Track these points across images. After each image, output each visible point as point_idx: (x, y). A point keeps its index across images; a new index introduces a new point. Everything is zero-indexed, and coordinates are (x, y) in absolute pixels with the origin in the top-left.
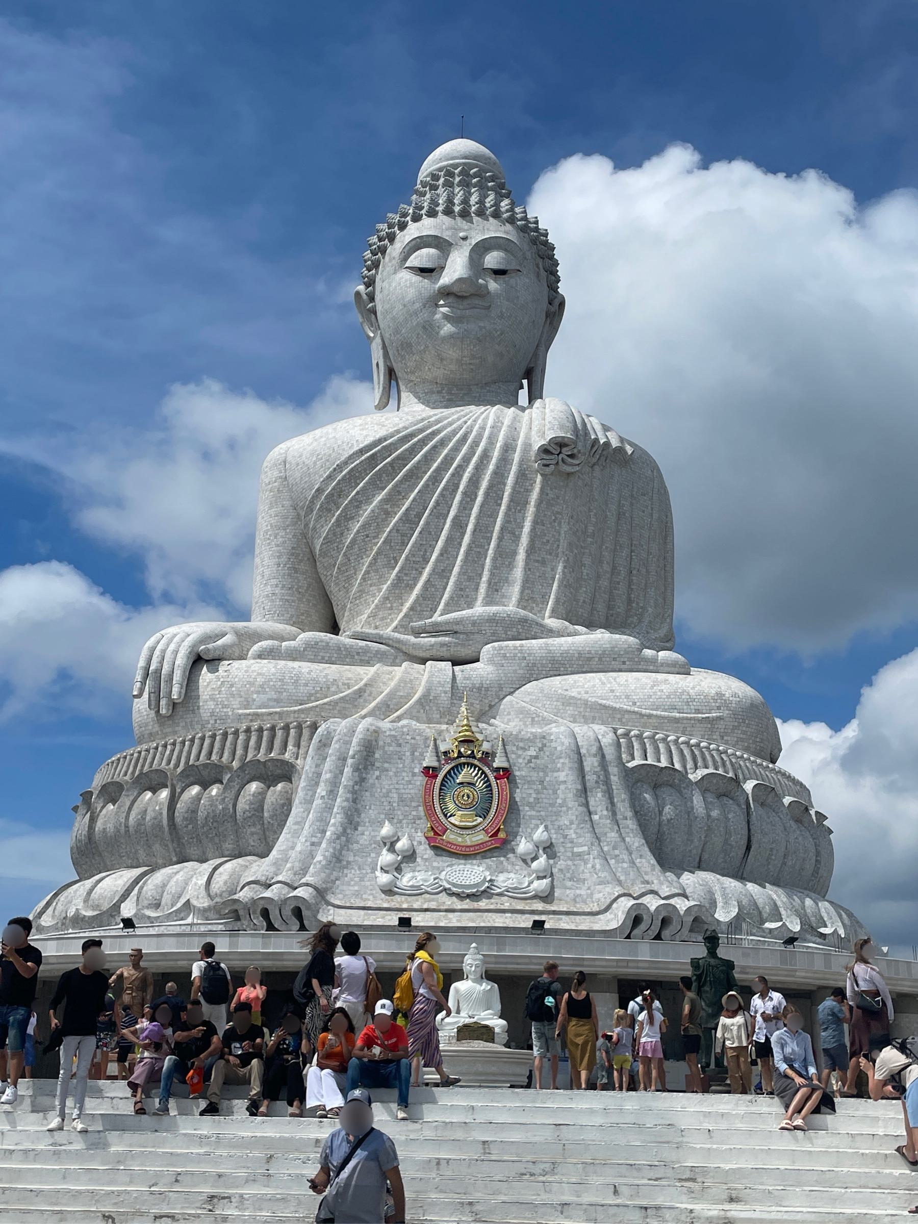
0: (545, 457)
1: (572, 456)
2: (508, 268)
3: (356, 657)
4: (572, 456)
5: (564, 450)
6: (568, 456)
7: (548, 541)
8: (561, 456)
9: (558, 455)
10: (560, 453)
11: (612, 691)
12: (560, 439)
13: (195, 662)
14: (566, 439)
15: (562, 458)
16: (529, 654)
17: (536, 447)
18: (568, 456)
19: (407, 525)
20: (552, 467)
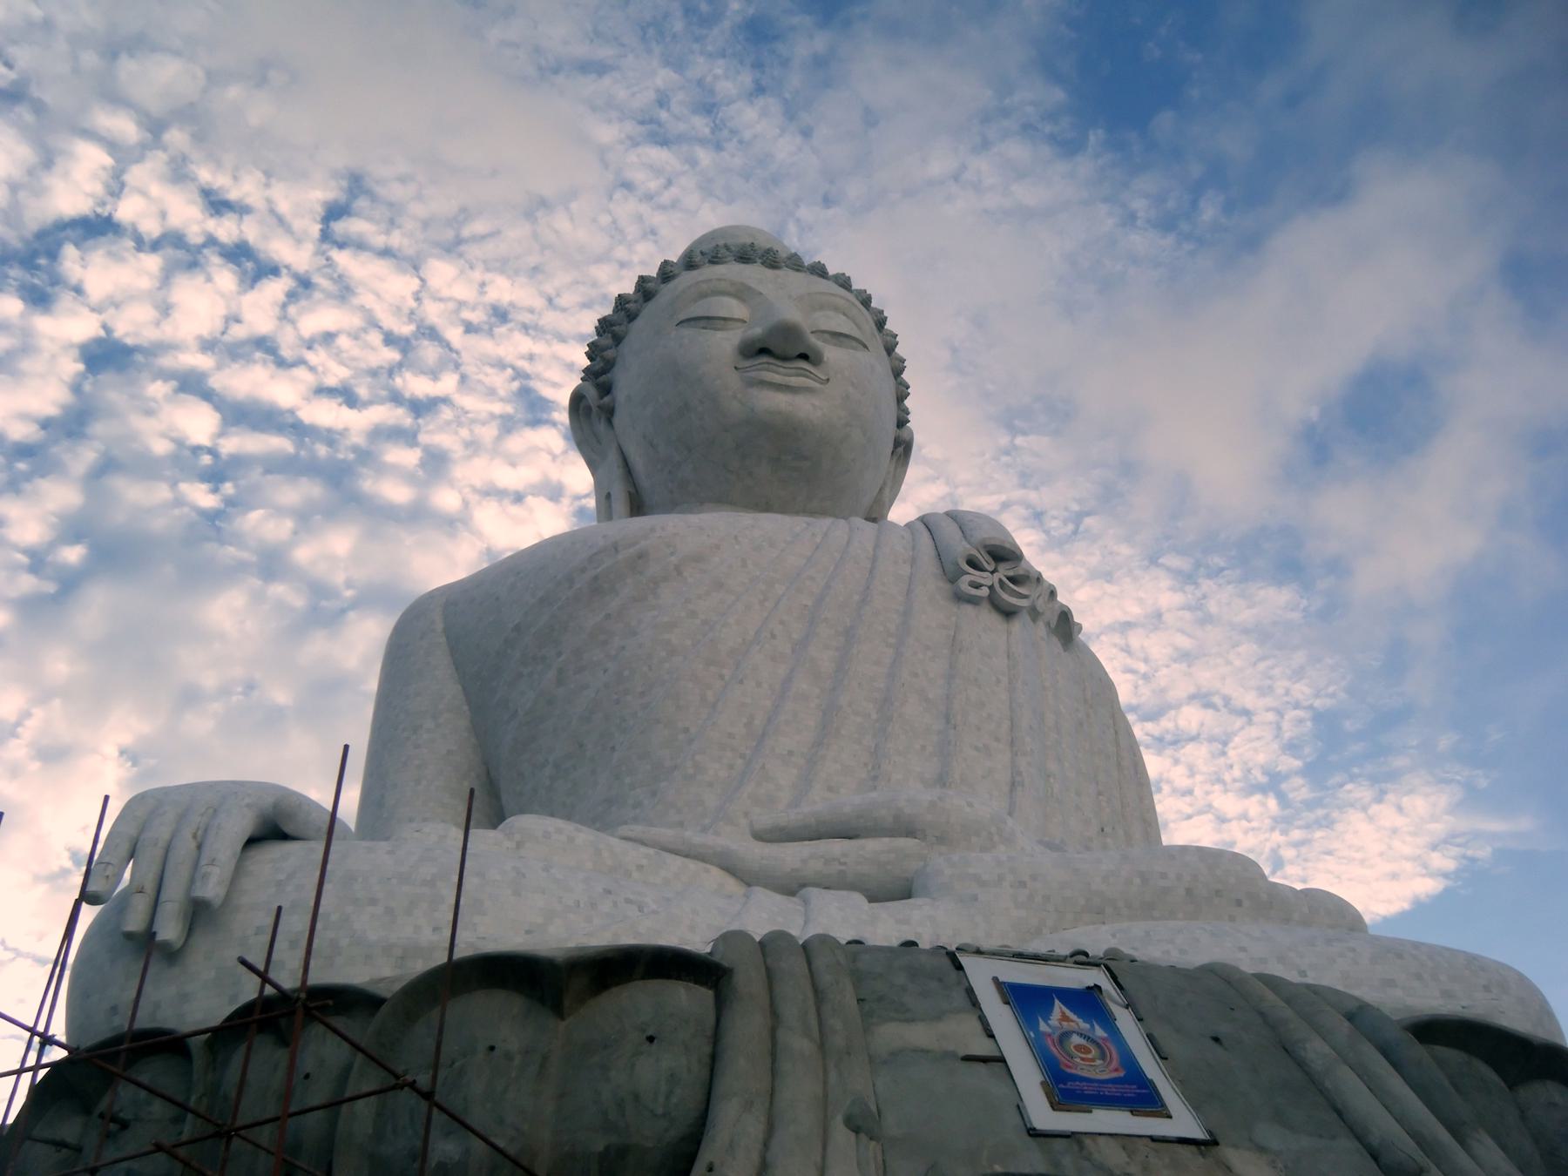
1: (1012, 580)
3: (636, 875)
4: (1012, 580)
6: (1011, 579)
9: (992, 573)
11: (1243, 949)
13: (252, 842)
15: (1000, 580)
16: (1034, 878)
18: (1011, 579)
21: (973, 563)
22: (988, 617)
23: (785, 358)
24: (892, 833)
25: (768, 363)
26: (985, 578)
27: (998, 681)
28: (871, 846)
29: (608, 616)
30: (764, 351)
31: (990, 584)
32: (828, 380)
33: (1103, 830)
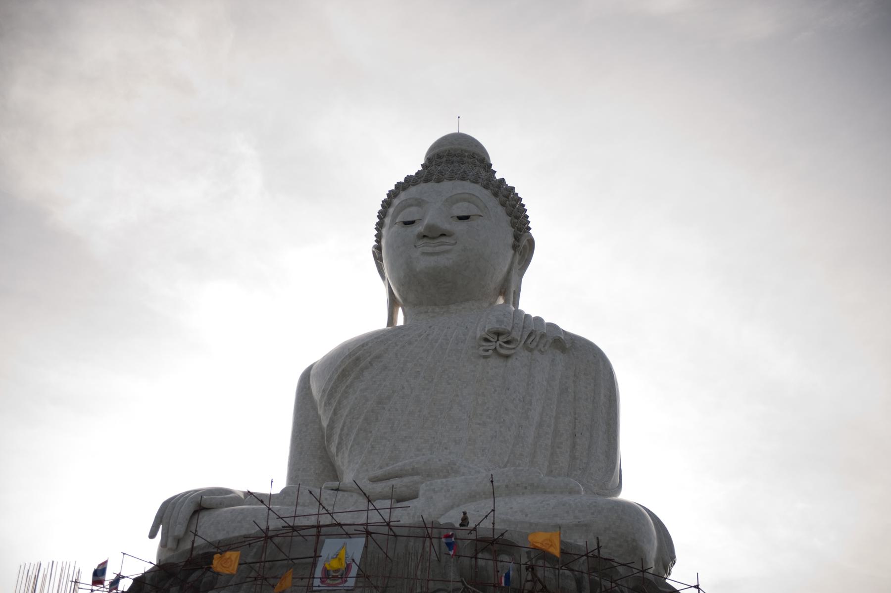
0: (484, 344)
1: (507, 342)
2: (469, 215)
5: (501, 338)
7: (488, 408)
8: (498, 343)
9: (496, 342)
10: (498, 340)
12: (495, 330)
14: (500, 330)
17: (478, 336)
19: (380, 406)
20: (491, 352)
21: (486, 340)
22: (494, 361)
23: (434, 238)
24: (412, 475)
25: (426, 243)
26: (492, 346)
27: (495, 391)
28: (406, 480)
29: (347, 387)
30: (424, 236)
31: (493, 347)
32: (456, 242)
33: (575, 435)
